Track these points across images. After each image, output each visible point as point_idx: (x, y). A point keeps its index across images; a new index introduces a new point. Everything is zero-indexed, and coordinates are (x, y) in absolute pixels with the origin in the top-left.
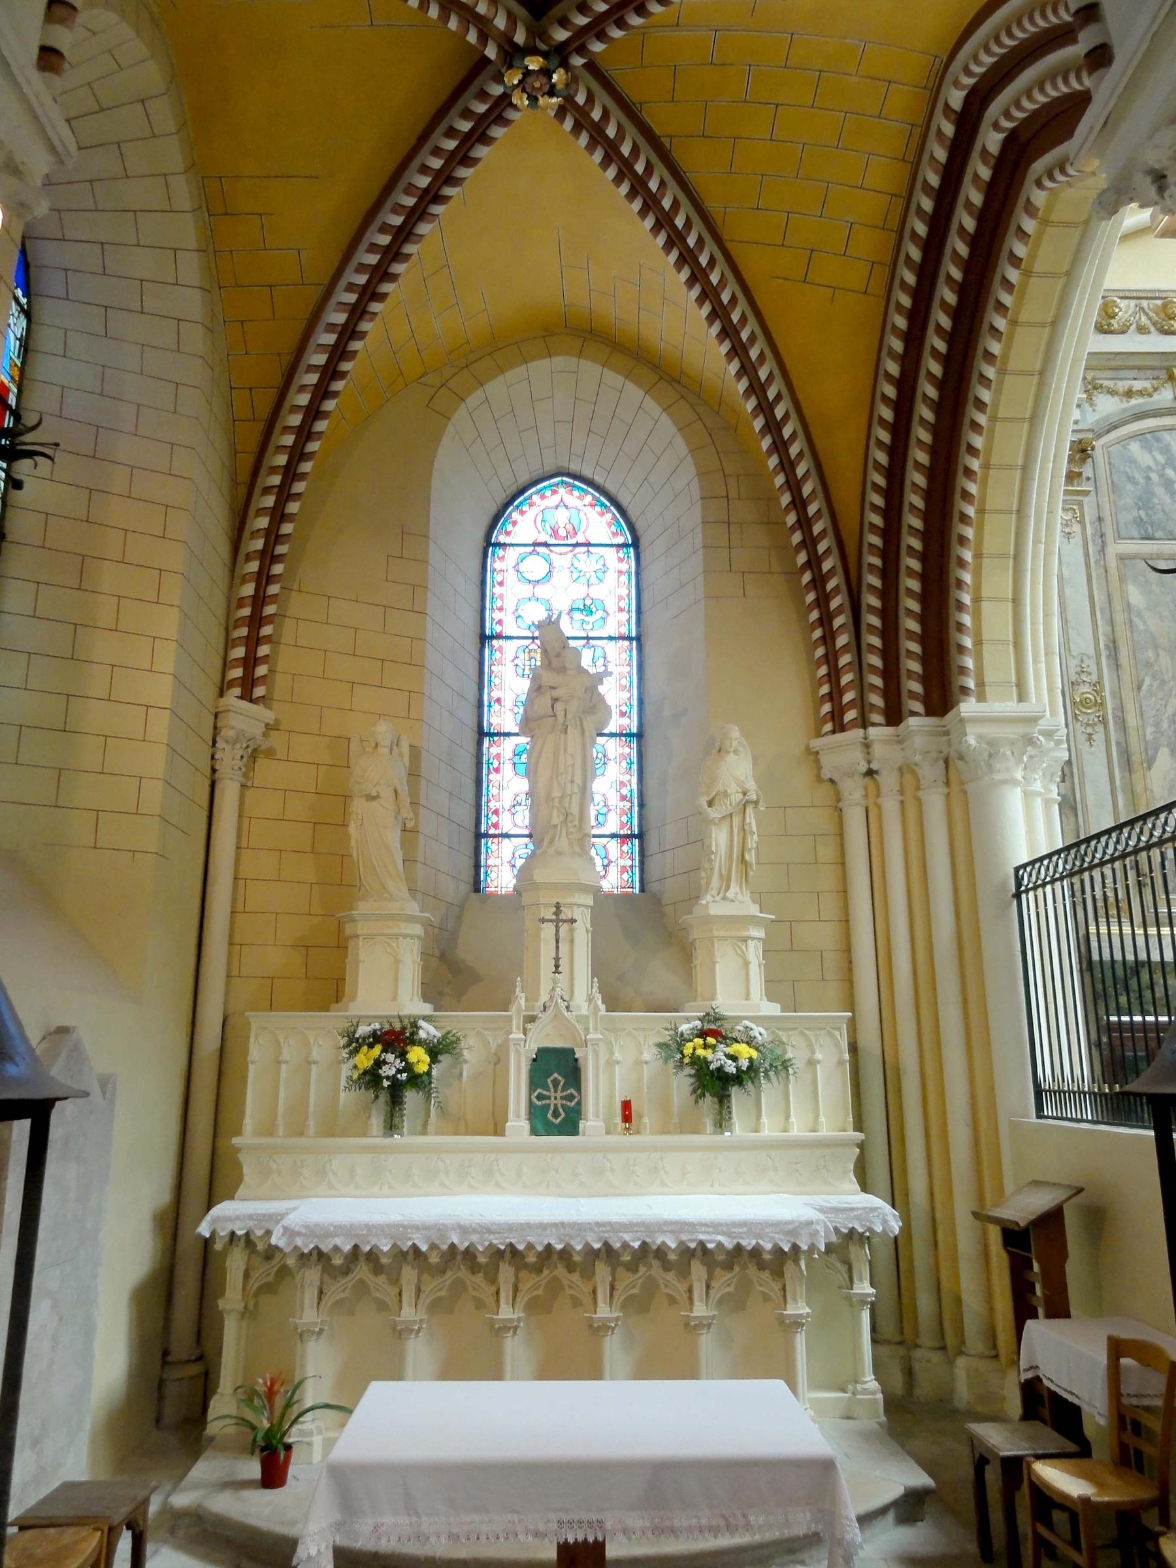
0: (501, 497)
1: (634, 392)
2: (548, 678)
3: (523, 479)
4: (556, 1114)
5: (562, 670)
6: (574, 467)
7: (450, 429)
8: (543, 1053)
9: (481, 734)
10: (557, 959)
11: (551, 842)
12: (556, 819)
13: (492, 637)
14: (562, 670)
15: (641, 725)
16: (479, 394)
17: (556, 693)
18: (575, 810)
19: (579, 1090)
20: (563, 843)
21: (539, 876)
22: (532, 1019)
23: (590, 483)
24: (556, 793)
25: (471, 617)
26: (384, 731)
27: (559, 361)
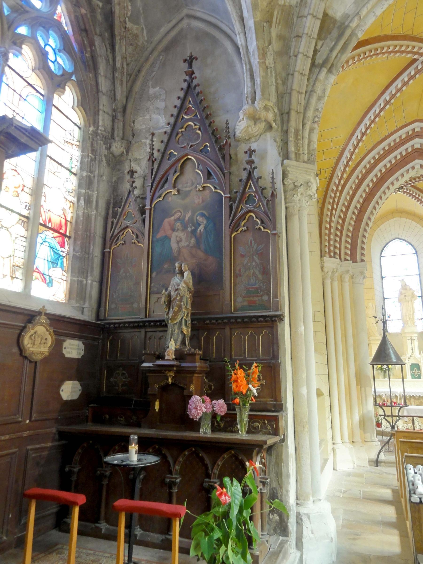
0: (383, 246)
1: (414, 223)
2: (403, 291)
3: (388, 241)
4: (416, 375)
5: (406, 289)
6: (400, 237)
7: (373, 238)
8: (412, 364)
9: (384, 299)
10: (412, 347)
11: (407, 324)
12: (408, 319)
13: (384, 277)
14: (406, 289)
15: (422, 294)
16: (379, 229)
17: (405, 294)
18: (412, 318)
19: (420, 370)
20: (409, 324)
21: (406, 331)
22: (409, 358)
23: (404, 240)
24: (407, 314)
25: (379, 274)
26: (370, 304)
27: (396, 219)
